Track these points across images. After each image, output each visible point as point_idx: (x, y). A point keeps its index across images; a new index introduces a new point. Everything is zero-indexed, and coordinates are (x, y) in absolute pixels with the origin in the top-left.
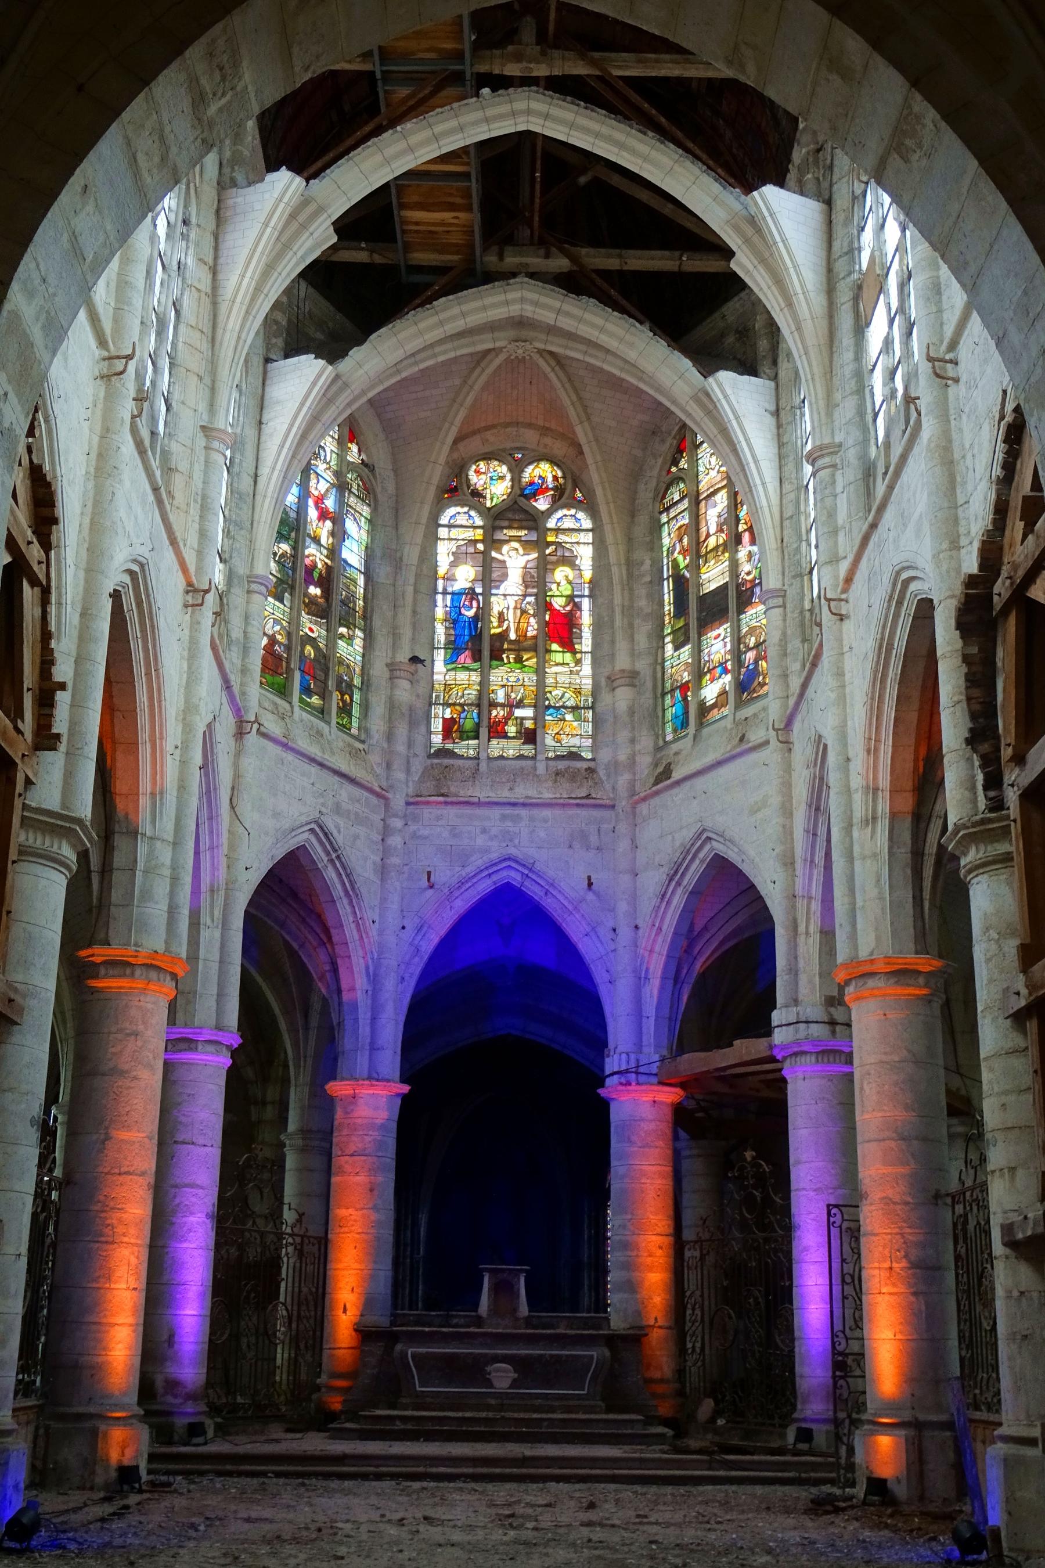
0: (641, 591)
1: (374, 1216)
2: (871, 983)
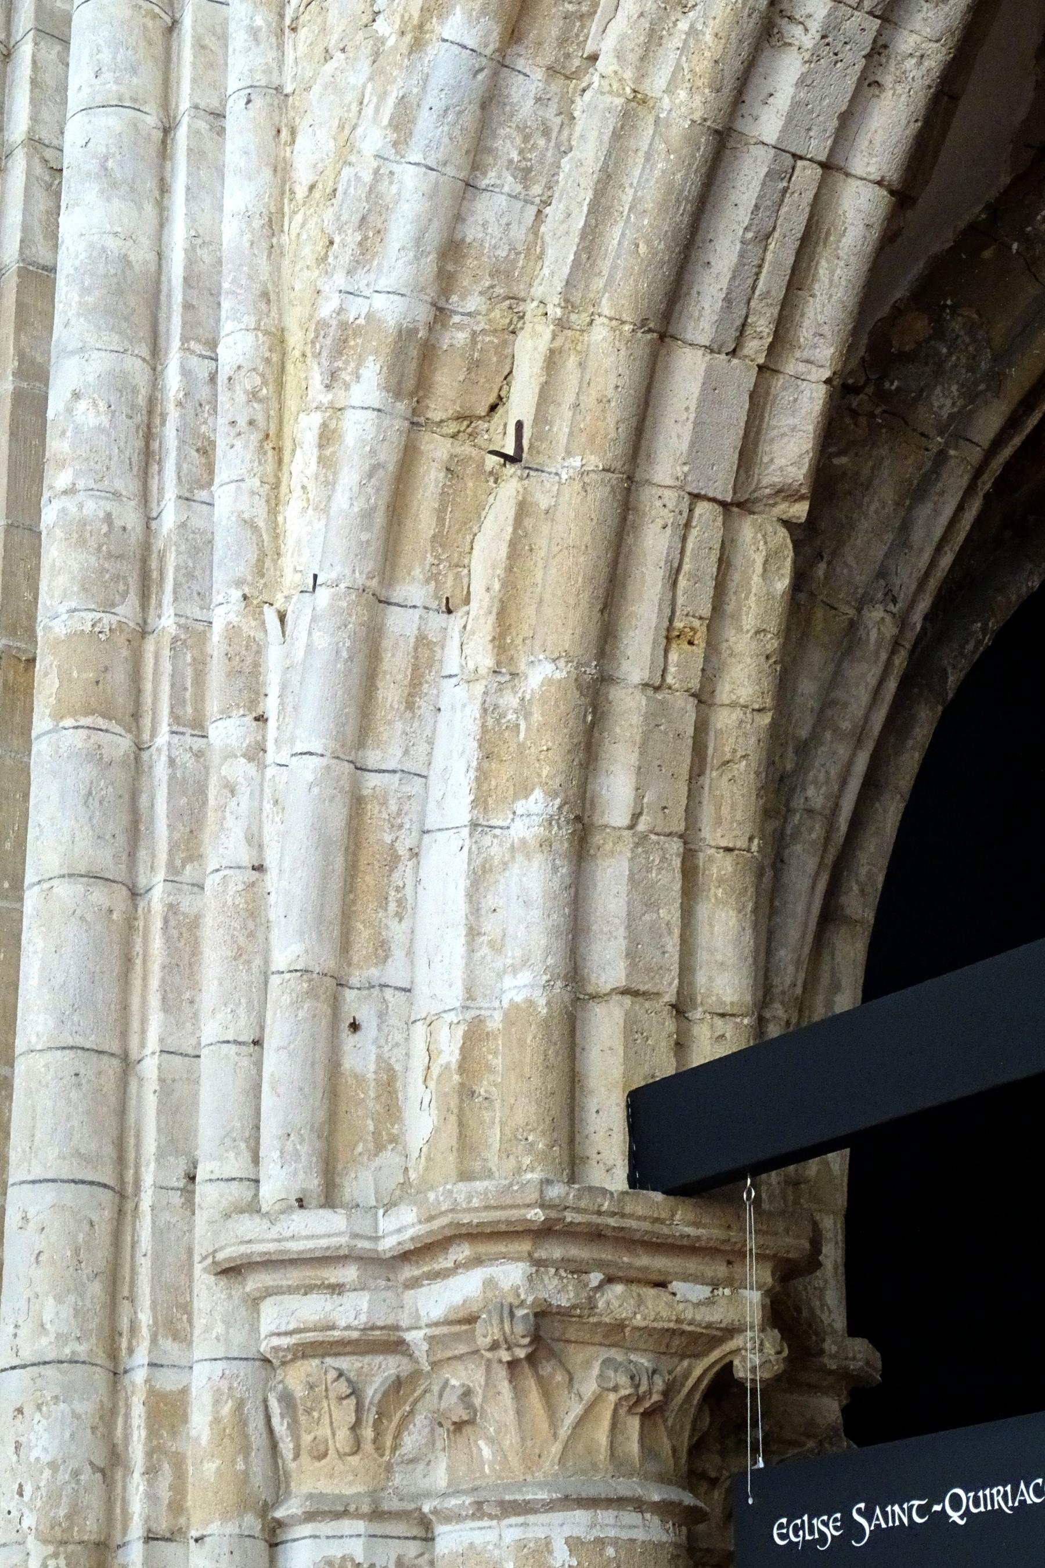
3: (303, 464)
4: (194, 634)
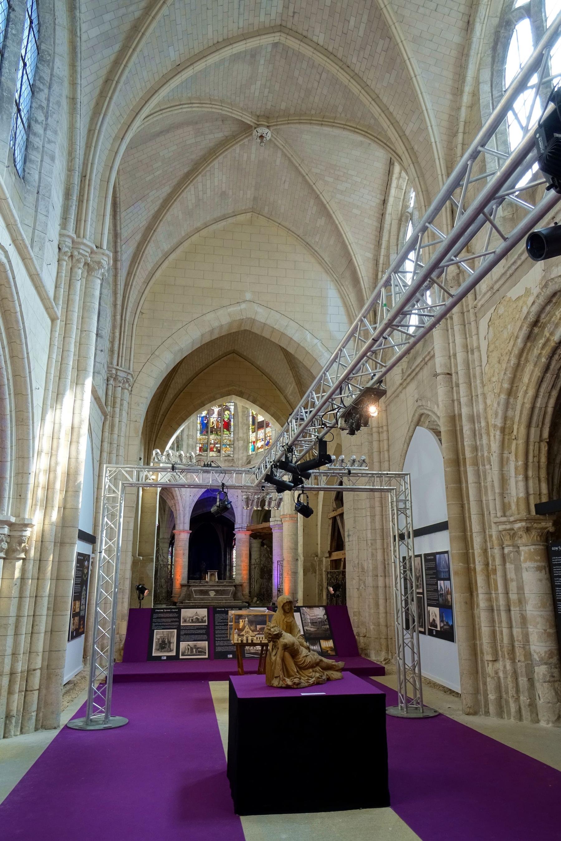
0: (245, 418)
1: (184, 560)
2: (287, 519)
3: (492, 438)
4: (483, 455)
